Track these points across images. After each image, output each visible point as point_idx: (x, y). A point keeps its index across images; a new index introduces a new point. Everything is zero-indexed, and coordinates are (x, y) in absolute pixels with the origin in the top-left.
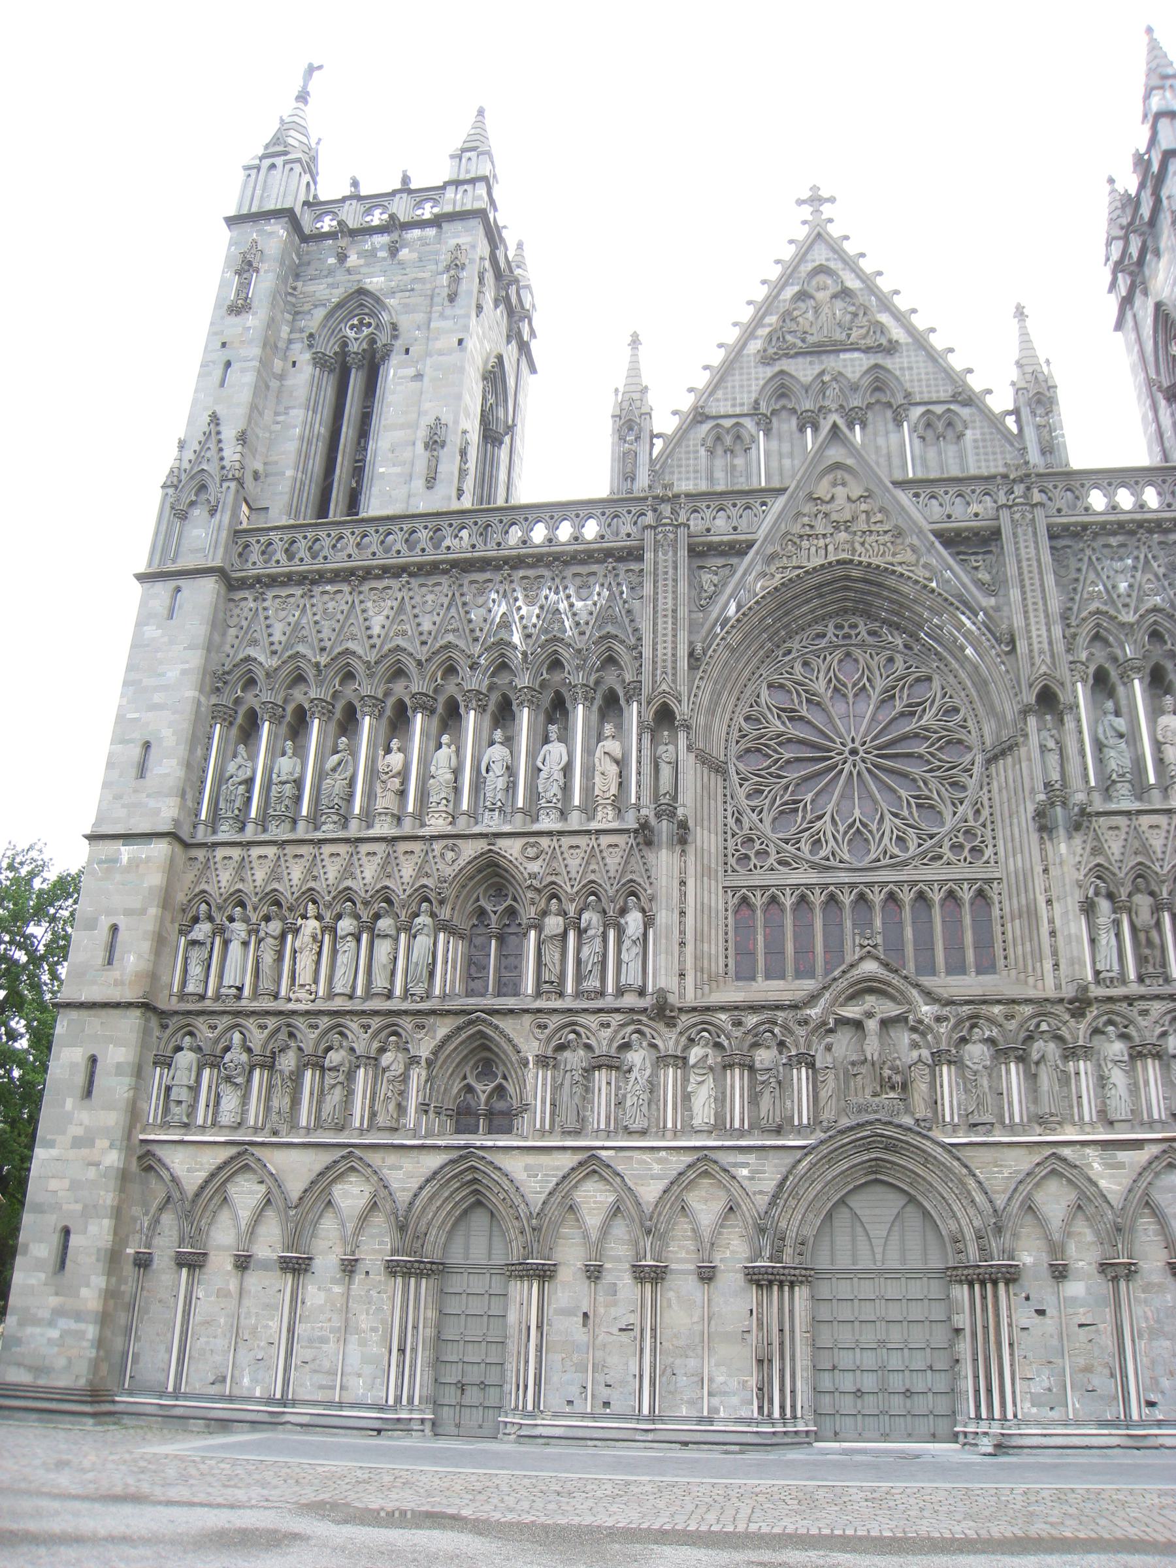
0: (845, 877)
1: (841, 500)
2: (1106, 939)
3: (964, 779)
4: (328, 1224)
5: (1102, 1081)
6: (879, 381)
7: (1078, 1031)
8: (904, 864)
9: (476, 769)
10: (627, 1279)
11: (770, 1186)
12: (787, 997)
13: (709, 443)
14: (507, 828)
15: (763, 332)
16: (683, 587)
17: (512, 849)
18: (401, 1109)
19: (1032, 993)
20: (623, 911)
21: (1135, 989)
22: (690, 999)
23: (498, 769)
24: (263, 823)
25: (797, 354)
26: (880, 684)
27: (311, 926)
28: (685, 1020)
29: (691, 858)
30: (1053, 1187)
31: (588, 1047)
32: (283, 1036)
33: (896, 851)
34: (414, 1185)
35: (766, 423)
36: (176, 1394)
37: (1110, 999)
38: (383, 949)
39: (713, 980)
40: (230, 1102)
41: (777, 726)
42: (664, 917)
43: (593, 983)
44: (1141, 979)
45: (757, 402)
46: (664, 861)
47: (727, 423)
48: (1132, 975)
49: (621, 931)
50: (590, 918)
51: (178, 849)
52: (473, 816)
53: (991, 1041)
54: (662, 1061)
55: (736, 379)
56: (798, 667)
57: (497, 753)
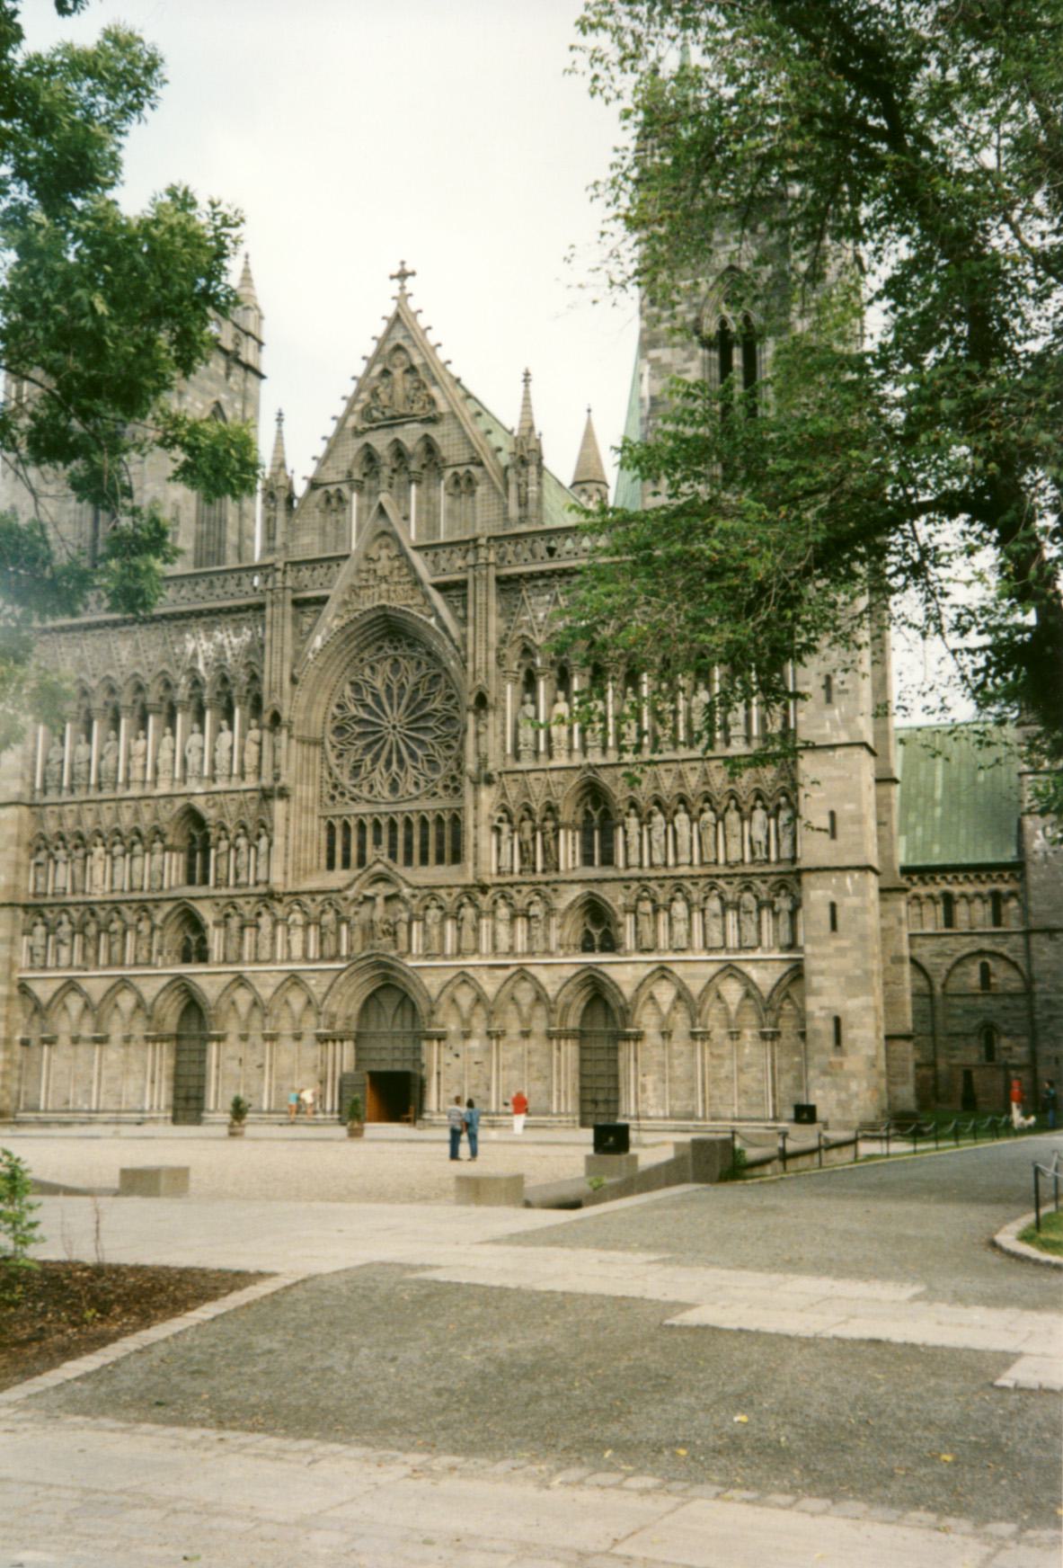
0: (383, 808)
1: (384, 561)
2: (506, 848)
3: (454, 743)
4: (116, 1017)
5: (494, 934)
6: (430, 447)
7: (484, 901)
8: (417, 798)
9: (183, 751)
10: (259, 1040)
11: (324, 989)
12: (341, 884)
13: (322, 505)
14: (199, 790)
15: (358, 407)
16: (289, 630)
17: (199, 803)
18: (150, 952)
19: (462, 881)
20: (259, 837)
21: (516, 878)
22: (290, 888)
23: (195, 751)
24: (72, 789)
25: (379, 428)
26: (412, 679)
27: (99, 851)
28: (287, 899)
29: (292, 805)
30: (465, 989)
31: (241, 915)
32: (88, 916)
33: (412, 789)
34: (154, 993)
35: (358, 487)
36: (46, 1111)
37: (499, 885)
38: (137, 862)
39: (307, 872)
40: (64, 952)
41: (354, 710)
42: (278, 841)
43: (243, 879)
44: (521, 872)
45: (350, 474)
46: (279, 806)
47: (332, 489)
48: (516, 869)
49: (257, 848)
50: (242, 842)
51: (24, 810)
52: (184, 780)
53: (440, 908)
54: (275, 923)
55: (340, 450)
56: (367, 671)
57: (195, 739)
